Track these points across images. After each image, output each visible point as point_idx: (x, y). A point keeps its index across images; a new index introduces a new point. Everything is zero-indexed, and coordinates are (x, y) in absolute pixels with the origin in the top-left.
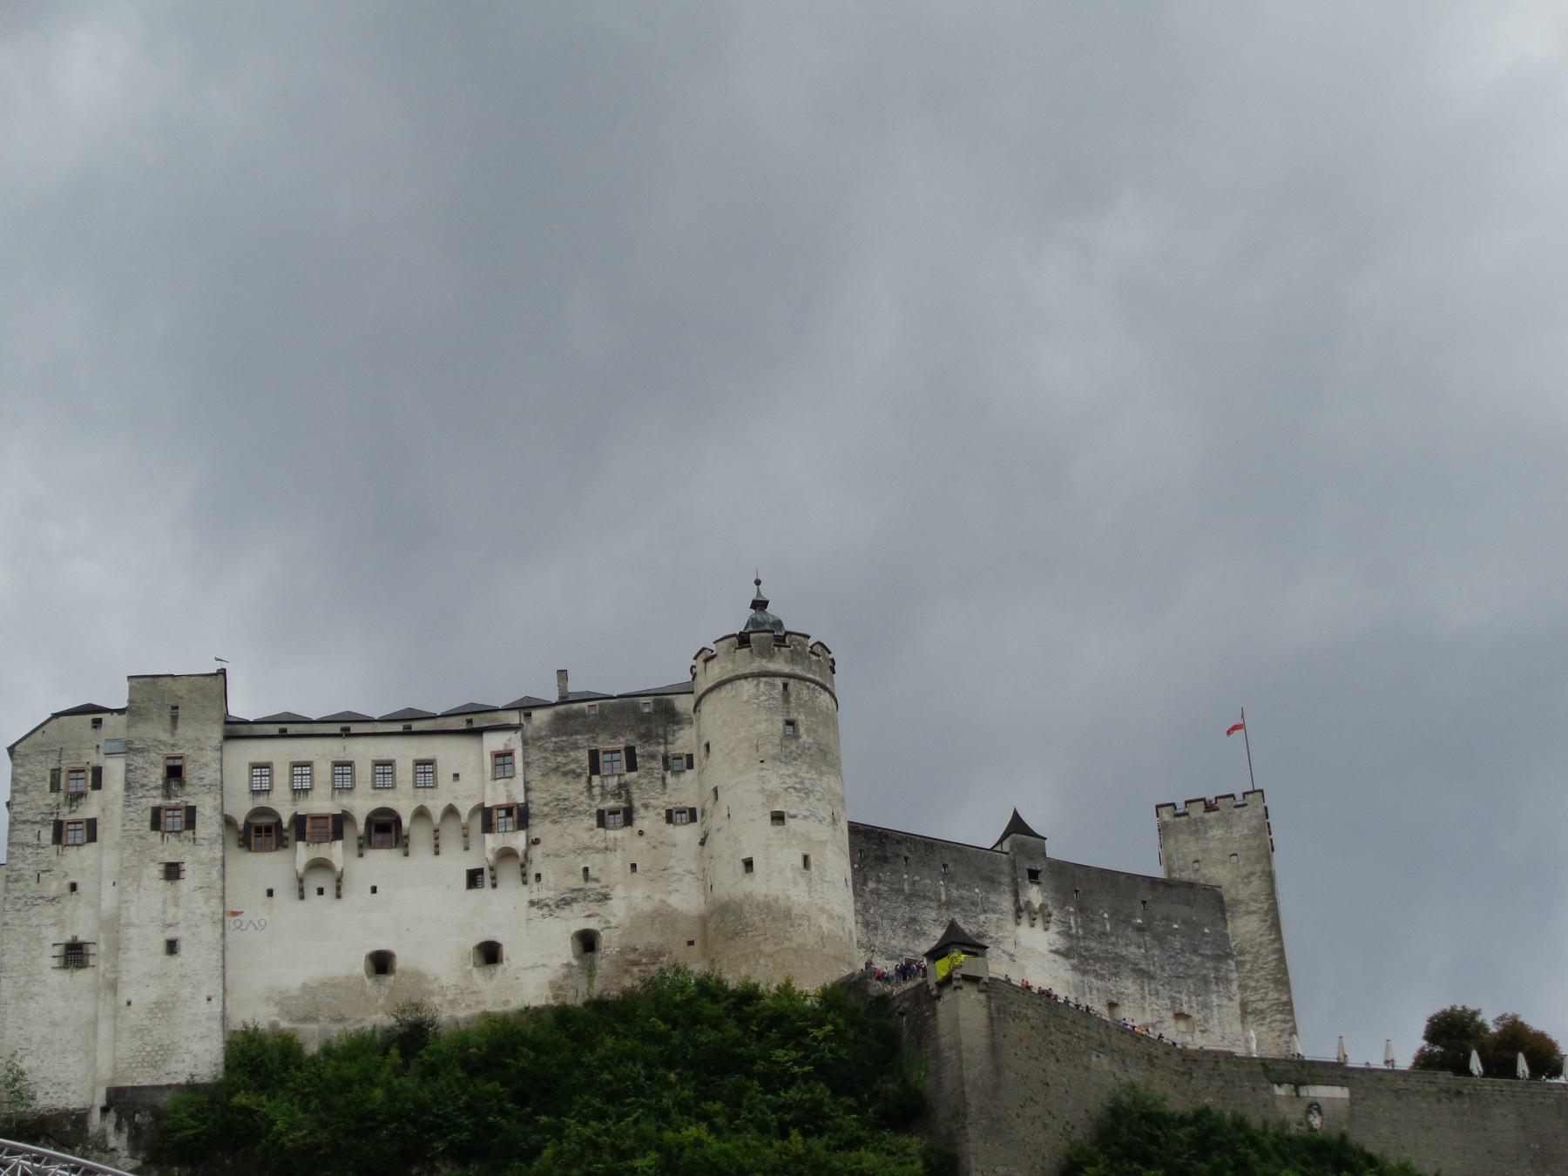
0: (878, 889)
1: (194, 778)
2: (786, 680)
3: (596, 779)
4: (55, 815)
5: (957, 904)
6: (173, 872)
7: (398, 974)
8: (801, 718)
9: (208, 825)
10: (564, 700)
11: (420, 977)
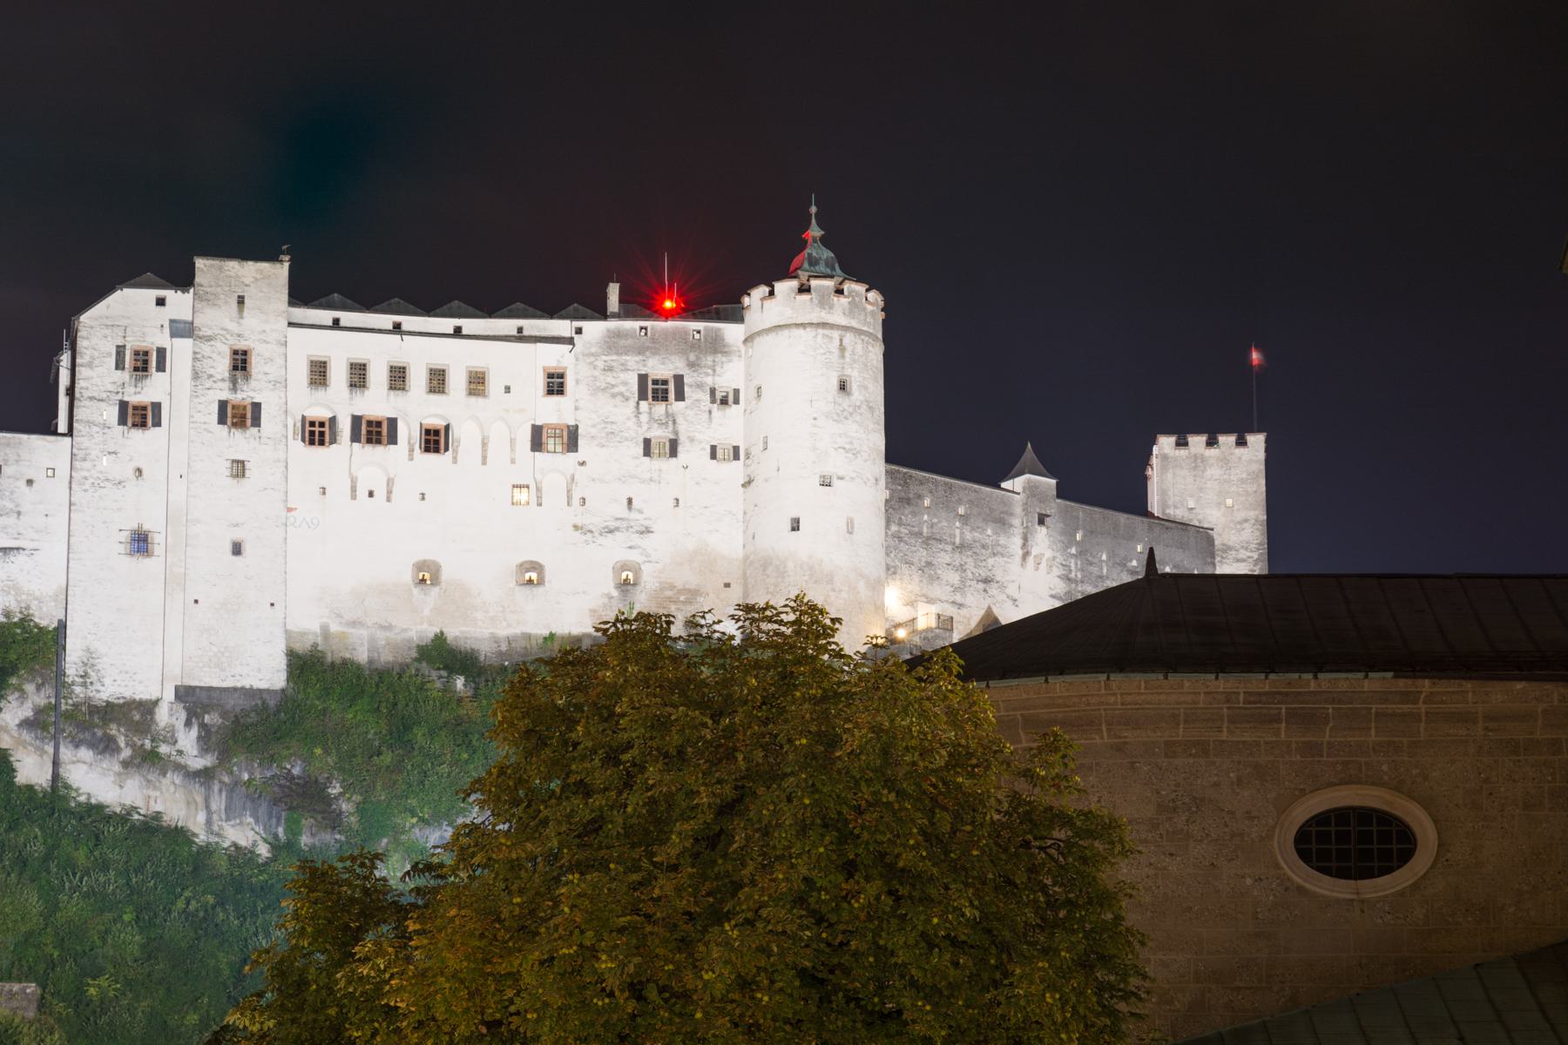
0: (899, 531)
1: (259, 372)
3: (644, 404)
4: (120, 395)
5: (970, 547)
6: (239, 469)
7: (443, 585)
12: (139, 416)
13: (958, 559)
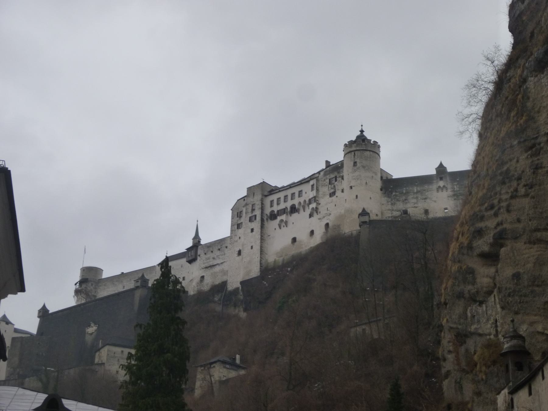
2: (354, 152)
3: (330, 186)
6: (252, 230)
8: (358, 161)
9: (259, 218)
10: (327, 167)
12: (239, 226)
13: (415, 196)
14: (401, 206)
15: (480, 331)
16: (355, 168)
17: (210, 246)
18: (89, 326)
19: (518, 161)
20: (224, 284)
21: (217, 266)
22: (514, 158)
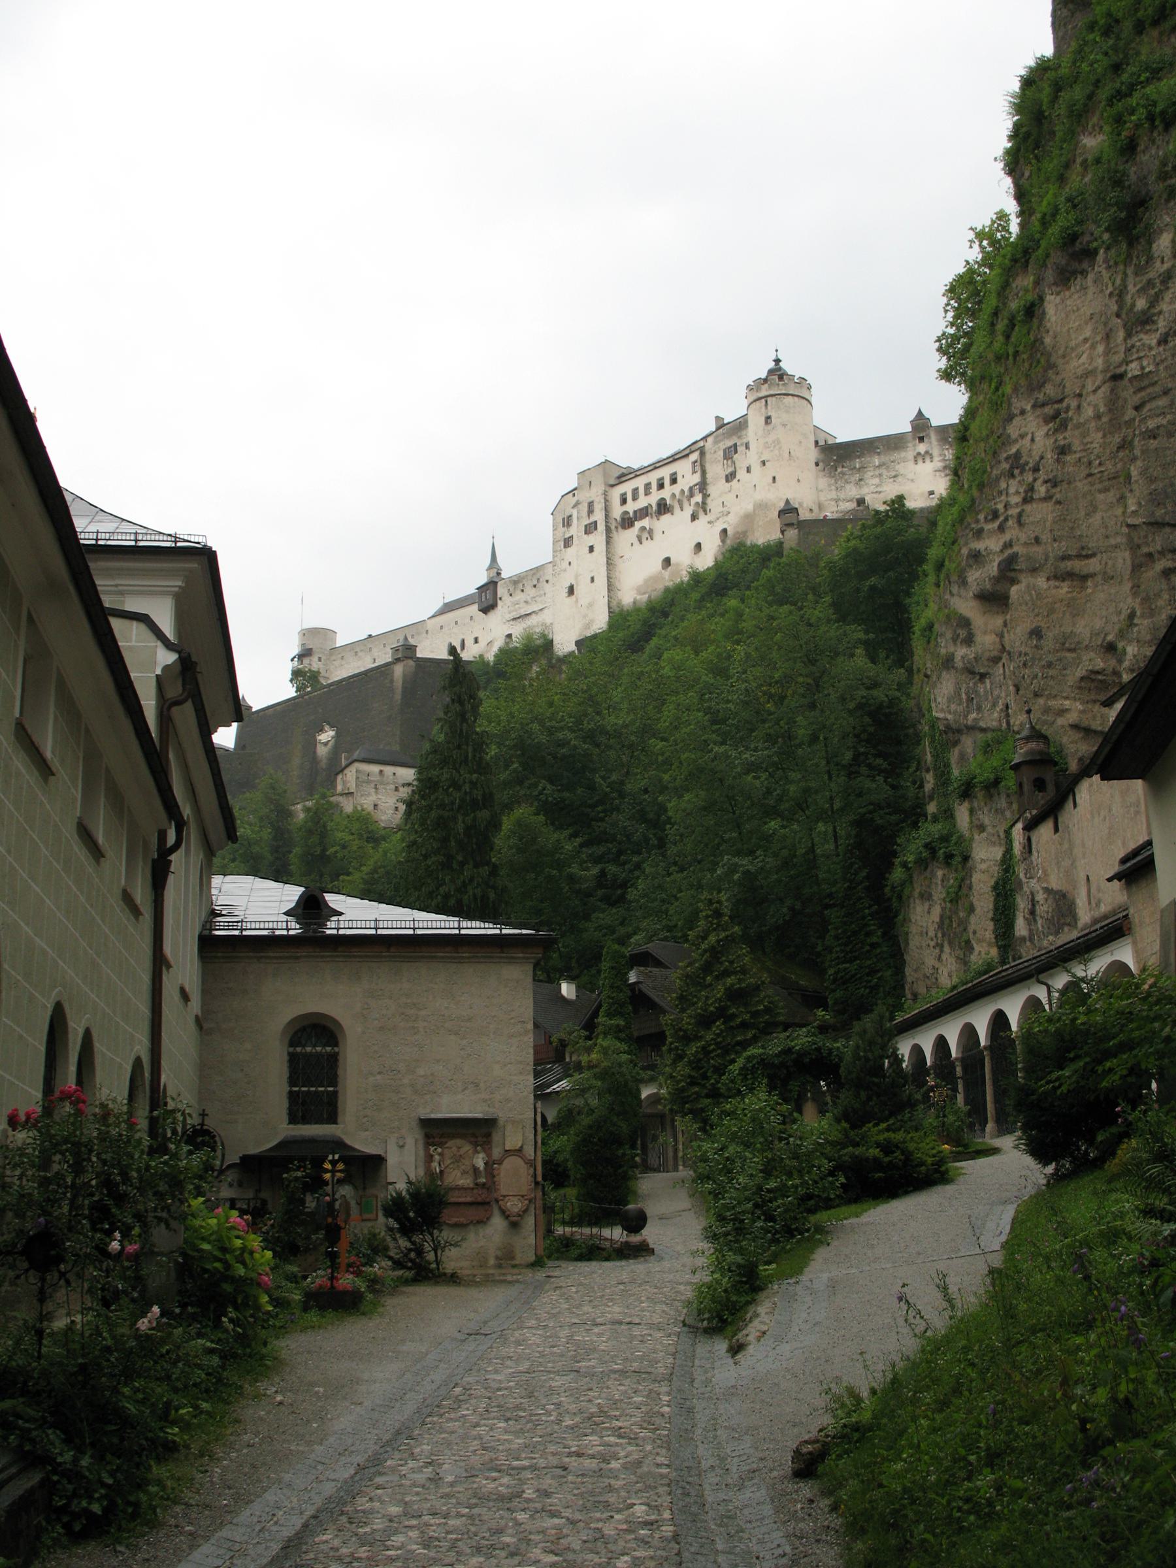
6: (591, 549)
9: (601, 527)
10: (717, 429)
11: (678, 564)
12: (568, 542)
13: (877, 472)
14: (853, 492)
15: (982, 724)
16: (770, 427)
17: (517, 582)
18: (322, 730)
19: (1033, 440)
20: (549, 644)
21: (533, 616)
22: (1027, 434)
